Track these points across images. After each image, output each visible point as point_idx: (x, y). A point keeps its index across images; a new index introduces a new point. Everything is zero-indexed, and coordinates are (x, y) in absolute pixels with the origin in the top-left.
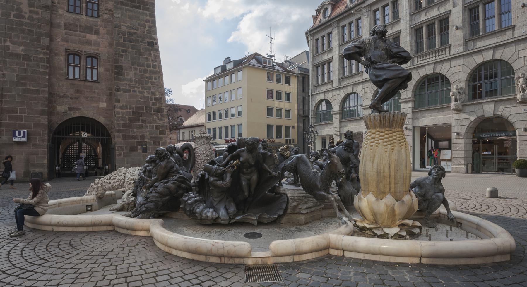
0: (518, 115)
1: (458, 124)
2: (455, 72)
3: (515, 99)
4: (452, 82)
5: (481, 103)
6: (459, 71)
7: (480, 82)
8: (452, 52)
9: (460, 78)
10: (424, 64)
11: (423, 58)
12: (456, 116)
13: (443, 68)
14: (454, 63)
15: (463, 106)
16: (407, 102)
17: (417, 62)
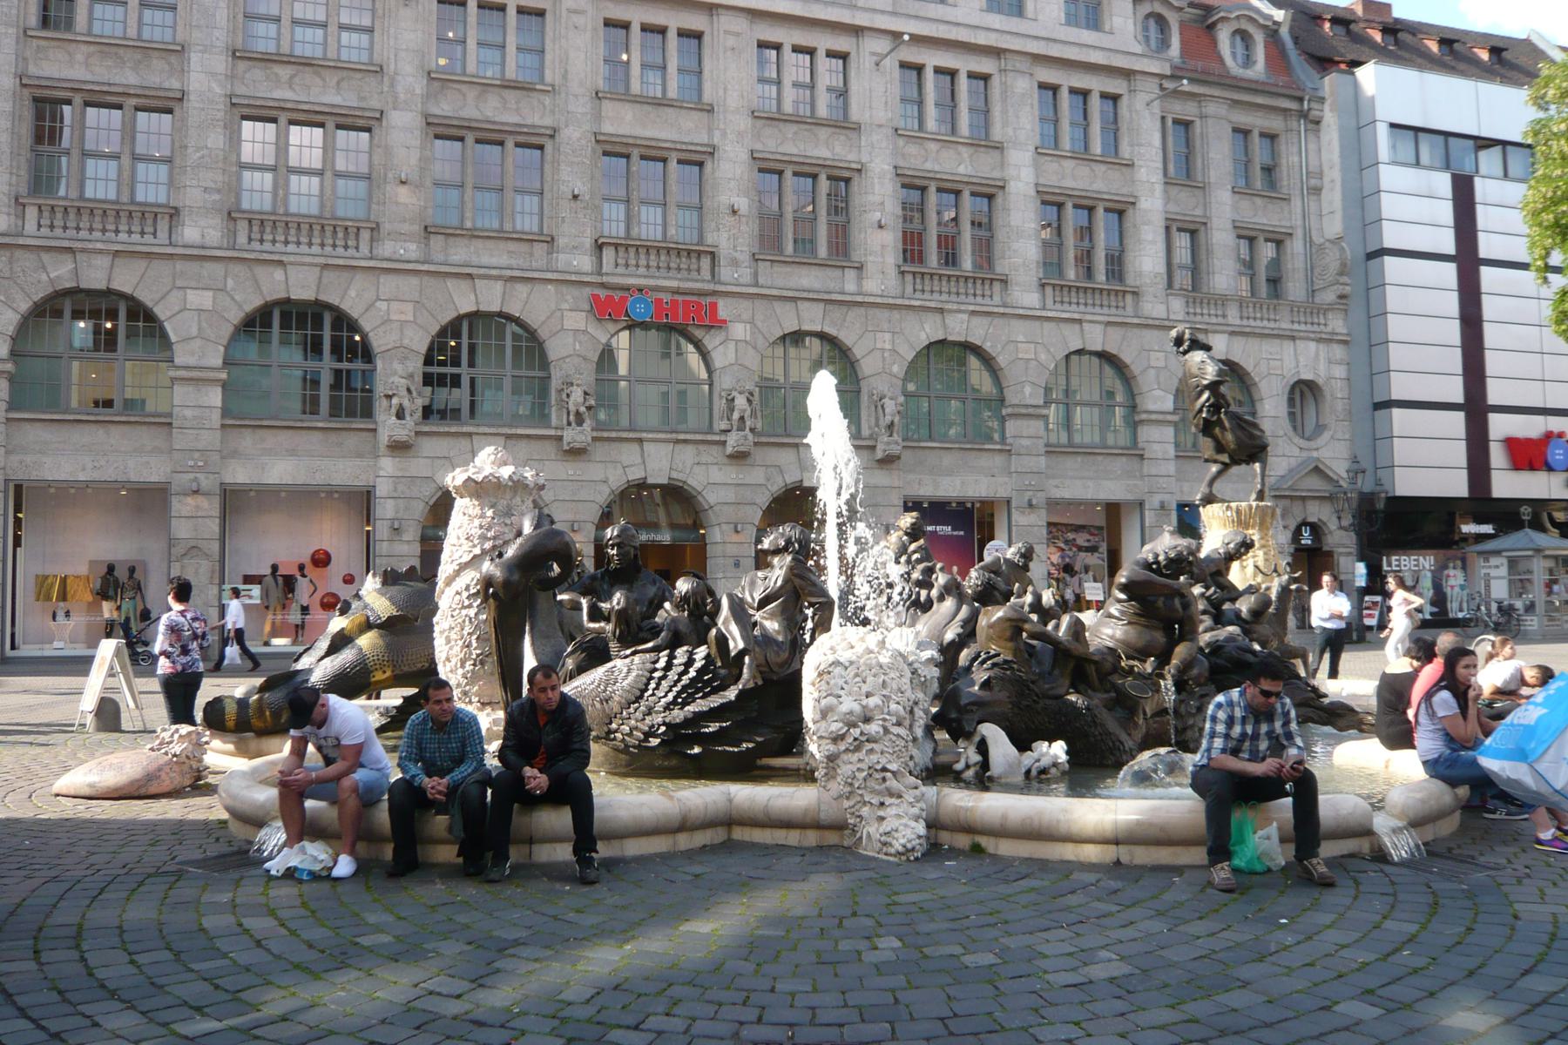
0: (559, 483)
1: (395, 490)
2: (393, 317)
3: (560, 438)
4: (383, 349)
5: (470, 435)
6: (403, 317)
7: (455, 370)
8: (387, 248)
9: (406, 342)
10: (284, 258)
11: (287, 235)
12: (388, 465)
13: (352, 293)
14: (389, 284)
15: (417, 433)
16: (198, 381)
17: (250, 240)
